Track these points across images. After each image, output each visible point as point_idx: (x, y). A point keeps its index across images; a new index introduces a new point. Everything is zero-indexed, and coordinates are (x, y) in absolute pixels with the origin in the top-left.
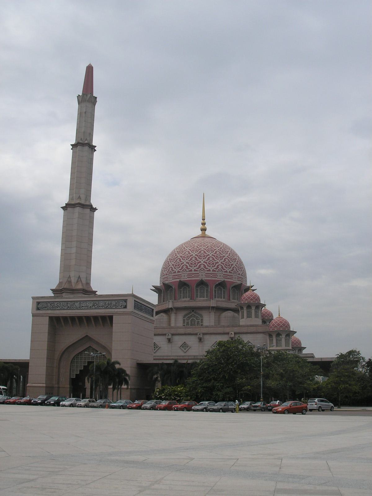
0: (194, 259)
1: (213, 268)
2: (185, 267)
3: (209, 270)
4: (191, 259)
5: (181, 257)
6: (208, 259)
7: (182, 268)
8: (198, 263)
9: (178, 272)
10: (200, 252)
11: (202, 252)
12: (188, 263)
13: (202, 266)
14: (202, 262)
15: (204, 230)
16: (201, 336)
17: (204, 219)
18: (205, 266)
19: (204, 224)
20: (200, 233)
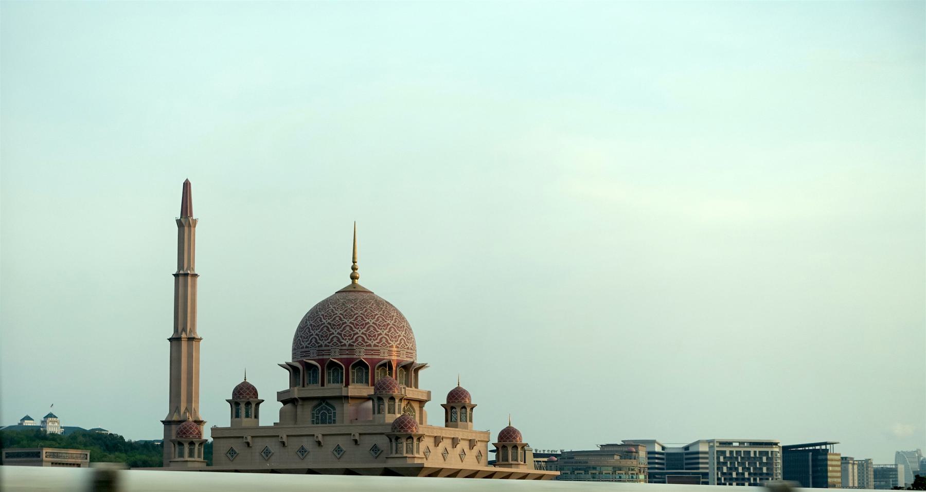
0: (348, 328)
1: (375, 342)
2: (335, 340)
3: (370, 345)
4: (344, 329)
5: (329, 324)
6: (368, 329)
7: (332, 340)
8: (355, 334)
9: (326, 346)
10: (356, 319)
11: (359, 318)
12: (340, 334)
13: (360, 340)
14: (360, 334)
15: (353, 278)
16: (357, 437)
17: (354, 262)
18: (363, 340)
19: (354, 269)
20: (350, 282)
